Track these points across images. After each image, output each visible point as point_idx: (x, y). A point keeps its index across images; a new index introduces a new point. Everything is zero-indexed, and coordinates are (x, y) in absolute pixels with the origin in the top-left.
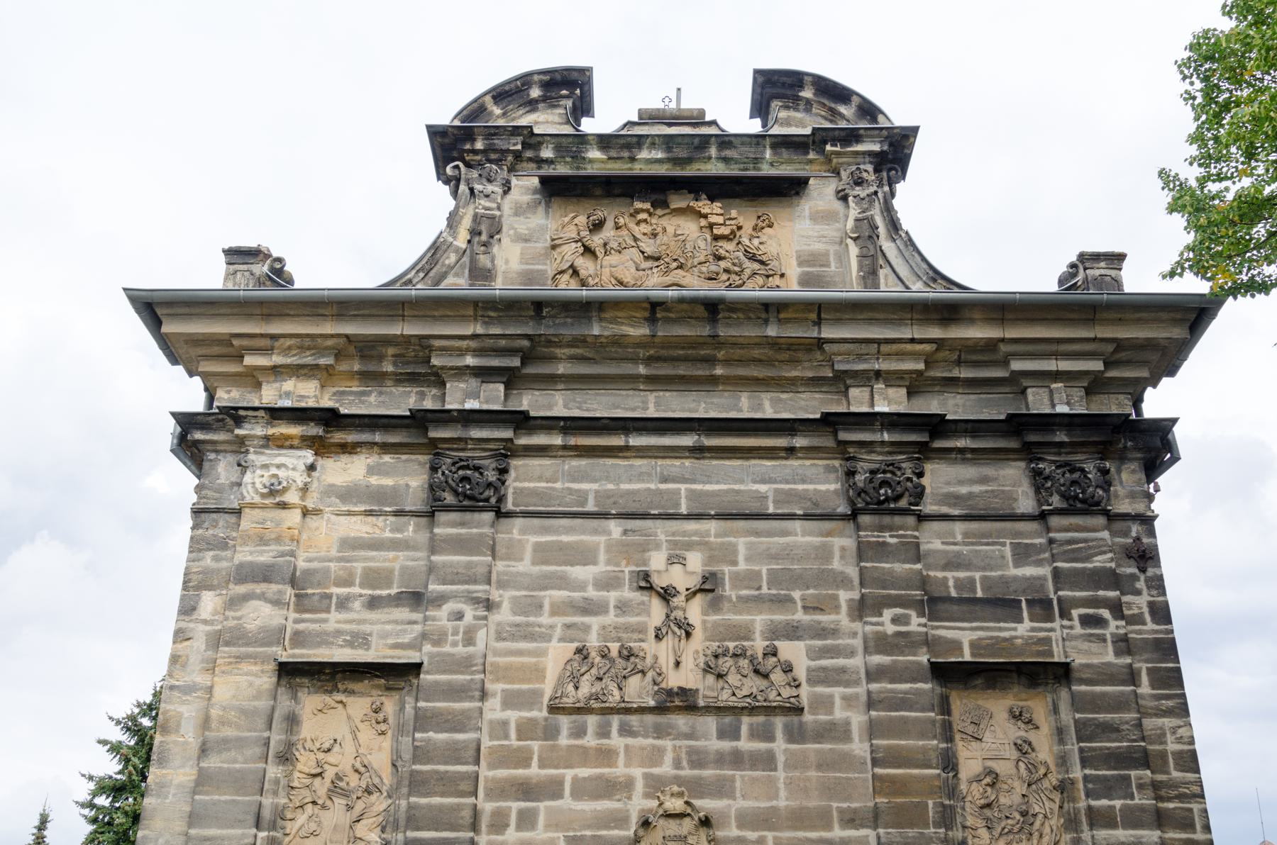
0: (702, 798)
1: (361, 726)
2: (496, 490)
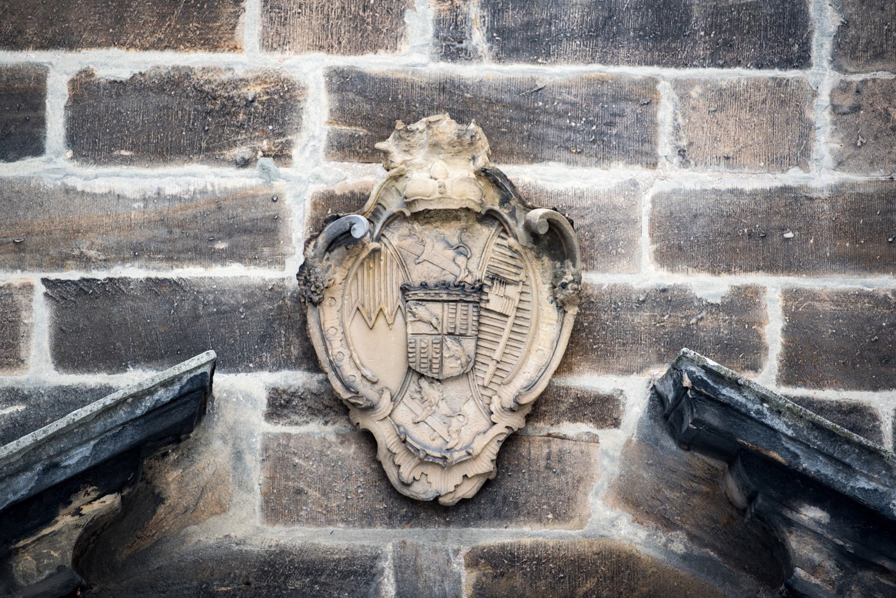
0: (534, 158)
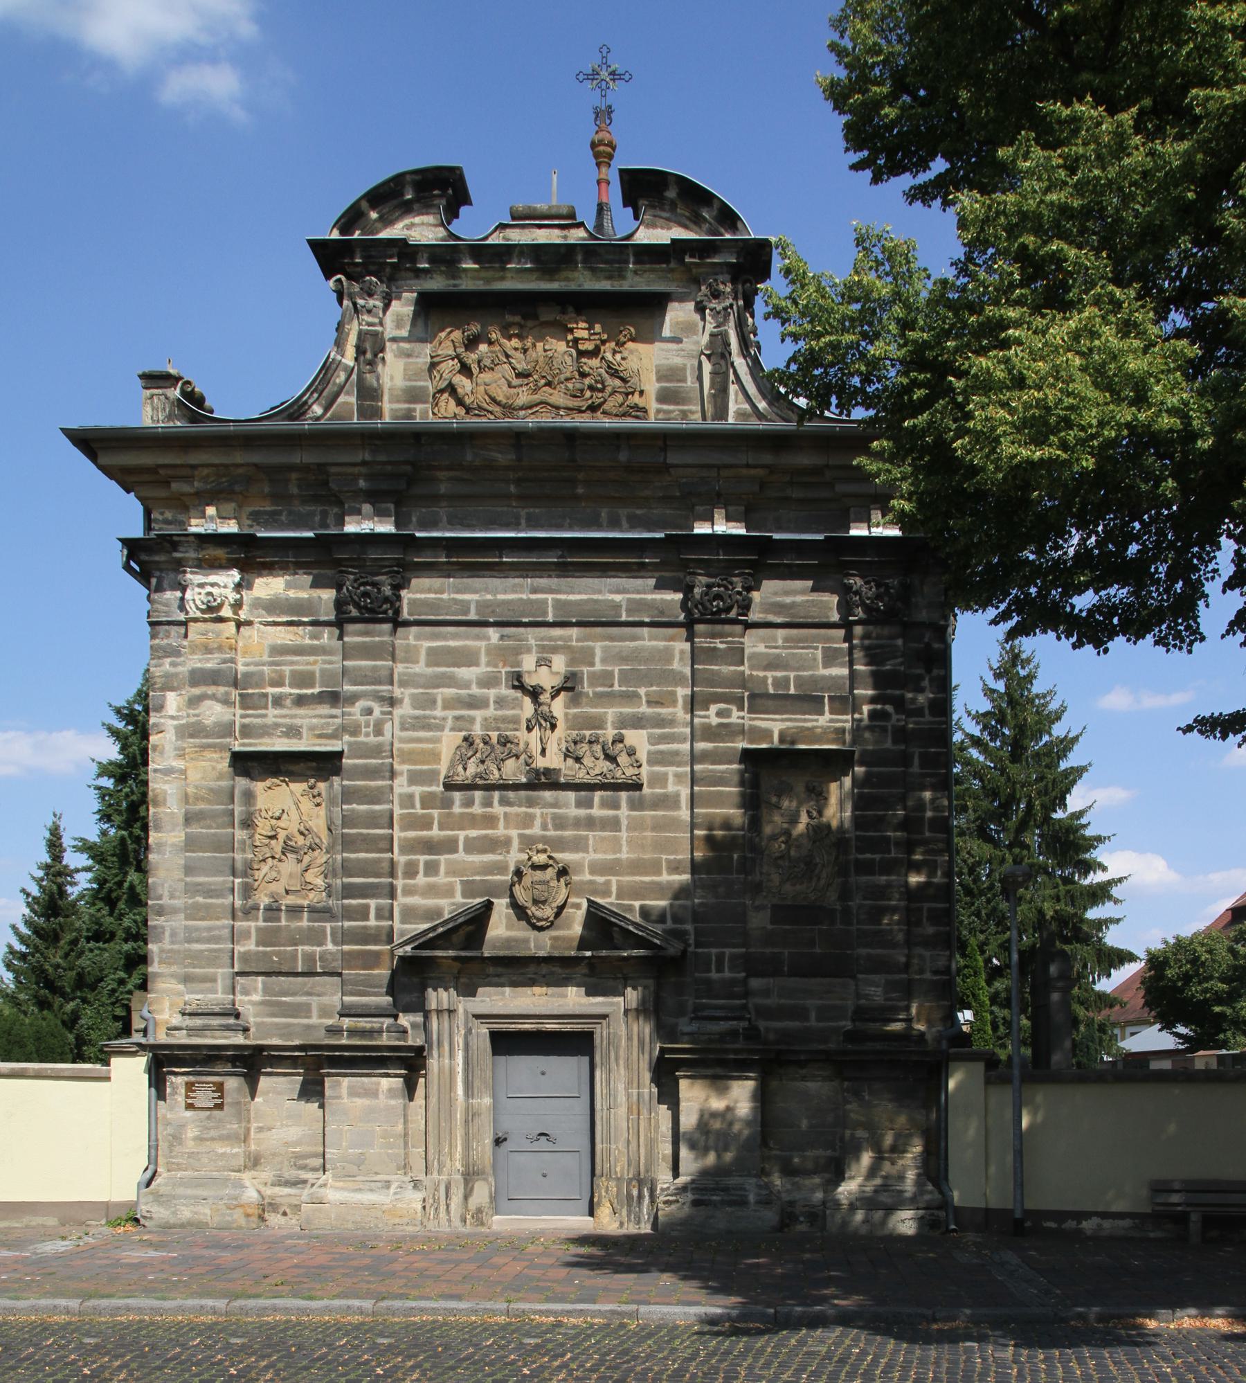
1: (301, 799)
2: (392, 604)
